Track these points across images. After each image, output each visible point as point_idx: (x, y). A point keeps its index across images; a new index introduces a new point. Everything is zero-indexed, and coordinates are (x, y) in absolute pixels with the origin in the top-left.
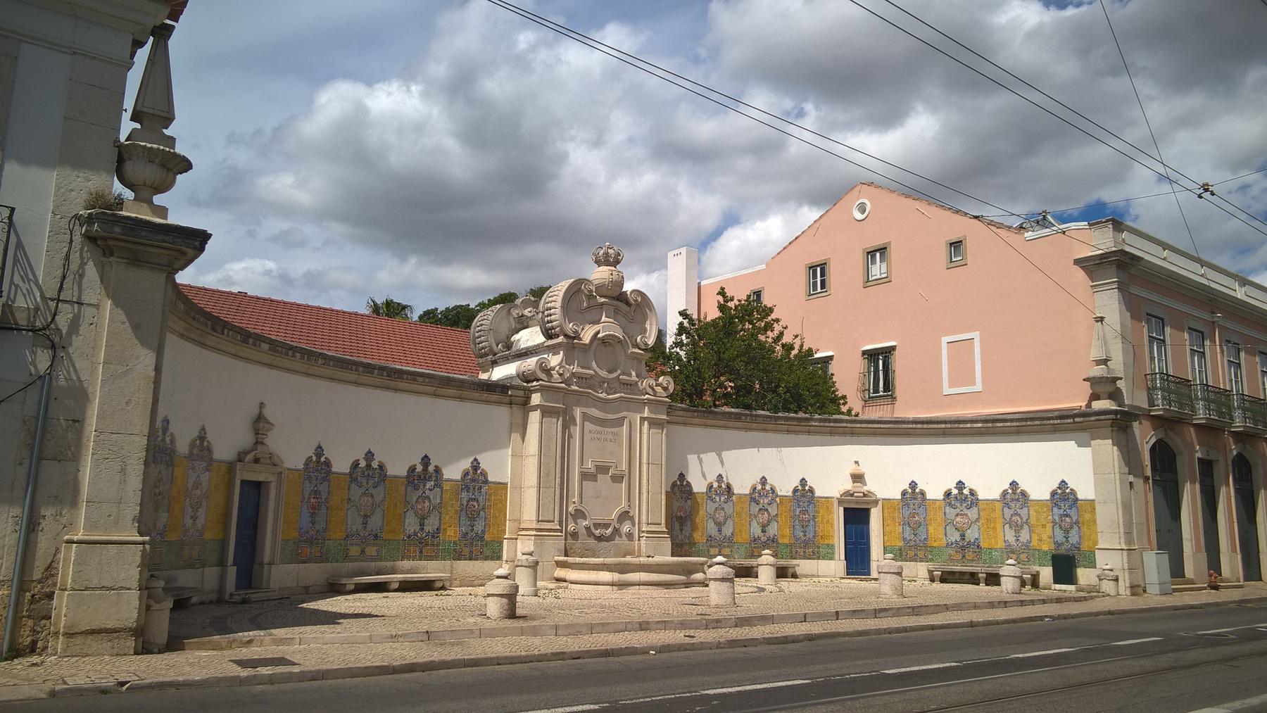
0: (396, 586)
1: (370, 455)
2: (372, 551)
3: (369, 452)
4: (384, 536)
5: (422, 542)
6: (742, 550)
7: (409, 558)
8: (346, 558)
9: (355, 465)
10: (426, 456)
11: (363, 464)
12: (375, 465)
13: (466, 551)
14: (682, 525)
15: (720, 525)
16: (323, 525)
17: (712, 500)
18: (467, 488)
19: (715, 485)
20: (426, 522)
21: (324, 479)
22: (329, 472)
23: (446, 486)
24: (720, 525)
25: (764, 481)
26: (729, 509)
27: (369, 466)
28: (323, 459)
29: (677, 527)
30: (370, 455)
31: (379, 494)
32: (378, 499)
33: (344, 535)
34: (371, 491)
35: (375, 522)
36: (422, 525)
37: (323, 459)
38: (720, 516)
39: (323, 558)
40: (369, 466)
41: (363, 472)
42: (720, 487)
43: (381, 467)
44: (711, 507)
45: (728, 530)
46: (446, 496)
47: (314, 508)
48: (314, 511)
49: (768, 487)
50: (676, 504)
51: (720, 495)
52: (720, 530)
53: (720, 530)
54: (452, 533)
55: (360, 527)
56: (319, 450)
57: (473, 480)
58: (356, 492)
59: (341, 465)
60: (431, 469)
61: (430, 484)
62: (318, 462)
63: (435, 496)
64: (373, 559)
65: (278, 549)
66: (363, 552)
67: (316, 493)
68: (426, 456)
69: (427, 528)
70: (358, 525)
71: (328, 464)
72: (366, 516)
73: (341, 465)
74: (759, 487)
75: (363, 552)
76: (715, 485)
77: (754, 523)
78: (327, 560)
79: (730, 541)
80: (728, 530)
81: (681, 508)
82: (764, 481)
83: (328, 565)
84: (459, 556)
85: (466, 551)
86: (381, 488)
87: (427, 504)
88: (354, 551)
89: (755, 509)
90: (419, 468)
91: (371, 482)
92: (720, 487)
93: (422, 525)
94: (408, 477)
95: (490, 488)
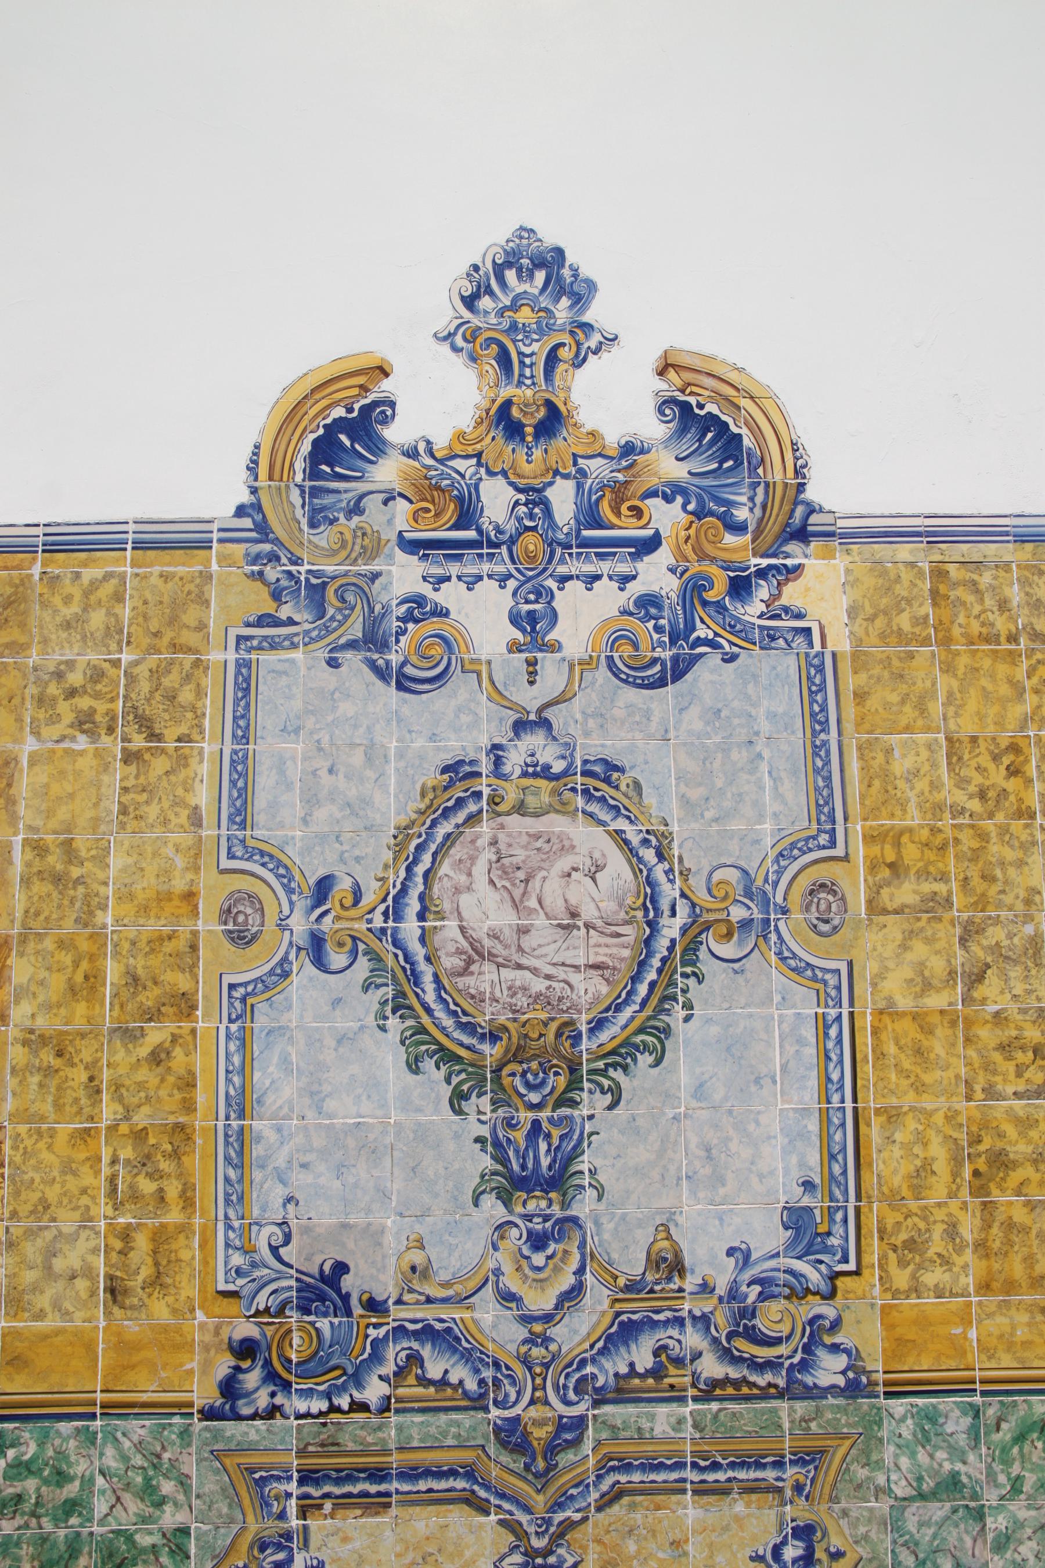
15: (531, 1087)
17: (405, 655)
24: (531, 1087)
26: (721, 766)
38: (535, 911)
42: (530, 424)
51: (535, 559)
52: (535, 1178)
53: (535, 1178)
76: (438, 401)
80: (710, 1153)
92: (530, 424)
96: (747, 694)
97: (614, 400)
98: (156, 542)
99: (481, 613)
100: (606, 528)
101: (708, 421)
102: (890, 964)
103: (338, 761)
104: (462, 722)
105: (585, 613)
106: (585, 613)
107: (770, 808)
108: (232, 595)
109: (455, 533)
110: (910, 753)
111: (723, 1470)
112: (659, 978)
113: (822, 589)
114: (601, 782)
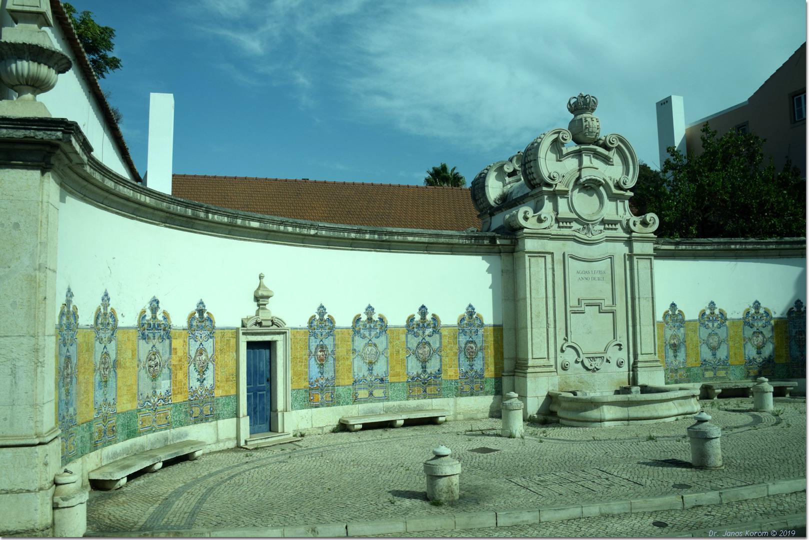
0: (402, 422)
1: (370, 310)
2: (378, 393)
3: (370, 307)
4: (389, 379)
5: (425, 383)
6: (738, 372)
7: (414, 397)
8: (356, 400)
9: (357, 319)
10: (423, 307)
11: (364, 318)
12: (375, 317)
13: (467, 388)
14: (675, 351)
15: (714, 350)
16: (332, 374)
17: (707, 327)
18: (464, 332)
19: (708, 312)
20: (428, 365)
21: (329, 334)
22: (332, 328)
23: (445, 332)
25: (757, 305)
26: (722, 333)
27: (370, 319)
28: (326, 317)
29: (671, 353)
31: (382, 342)
32: (381, 348)
33: (352, 381)
34: (374, 340)
35: (380, 368)
36: (424, 368)
37: (326, 317)
38: (714, 341)
39: (334, 401)
40: (370, 319)
41: (365, 326)
42: (713, 313)
43: (382, 319)
44: (704, 333)
45: (722, 354)
46: (445, 341)
47: (321, 360)
48: (321, 363)
49: (762, 311)
50: (669, 333)
51: (713, 321)
52: (714, 355)
53: (714, 355)
54: (451, 373)
55: (366, 374)
56: (322, 310)
57: (469, 325)
59: (343, 321)
60: (429, 317)
61: (428, 331)
62: (321, 320)
63: (435, 342)
64: (380, 400)
65: (290, 399)
66: (371, 394)
67: (323, 348)
68: (423, 307)
69: (429, 370)
70: (365, 371)
71: (331, 320)
72: (371, 364)
73: (343, 321)
74: (753, 311)
75: (371, 394)
76: (708, 312)
77: (749, 346)
78: (338, 404)
79: (725, 364)
80: (722, 354)
81: (674, 336)
82: (757, 305)
83: (340, 408)
84: (461, 393)
85: (467, 388)
86: (383, 338)
87: (427, 349)
88: (363, 394)
89: (749, 332)
90: (418, 317)
91: (373, 333)
92: (713, 313)
93: (424, 368)
94: (408, 326)
95: (486, 331)
96: (723, 329)
97: (717, 312)
98: (694, 321)
99: (710, 325)
100: (716, 320)
101: (722, 313)
102: (731, 343)
103: (704, 333)
104: (710, 331)
105: (716, 324)
106: (716, 324)
107: (725, 335)
108: (698, 324)
109: (709, 320)
110: (732, 332)
111: (723, 369)
112: (720, 344)
113: (727, 323)
114: (716, 334)
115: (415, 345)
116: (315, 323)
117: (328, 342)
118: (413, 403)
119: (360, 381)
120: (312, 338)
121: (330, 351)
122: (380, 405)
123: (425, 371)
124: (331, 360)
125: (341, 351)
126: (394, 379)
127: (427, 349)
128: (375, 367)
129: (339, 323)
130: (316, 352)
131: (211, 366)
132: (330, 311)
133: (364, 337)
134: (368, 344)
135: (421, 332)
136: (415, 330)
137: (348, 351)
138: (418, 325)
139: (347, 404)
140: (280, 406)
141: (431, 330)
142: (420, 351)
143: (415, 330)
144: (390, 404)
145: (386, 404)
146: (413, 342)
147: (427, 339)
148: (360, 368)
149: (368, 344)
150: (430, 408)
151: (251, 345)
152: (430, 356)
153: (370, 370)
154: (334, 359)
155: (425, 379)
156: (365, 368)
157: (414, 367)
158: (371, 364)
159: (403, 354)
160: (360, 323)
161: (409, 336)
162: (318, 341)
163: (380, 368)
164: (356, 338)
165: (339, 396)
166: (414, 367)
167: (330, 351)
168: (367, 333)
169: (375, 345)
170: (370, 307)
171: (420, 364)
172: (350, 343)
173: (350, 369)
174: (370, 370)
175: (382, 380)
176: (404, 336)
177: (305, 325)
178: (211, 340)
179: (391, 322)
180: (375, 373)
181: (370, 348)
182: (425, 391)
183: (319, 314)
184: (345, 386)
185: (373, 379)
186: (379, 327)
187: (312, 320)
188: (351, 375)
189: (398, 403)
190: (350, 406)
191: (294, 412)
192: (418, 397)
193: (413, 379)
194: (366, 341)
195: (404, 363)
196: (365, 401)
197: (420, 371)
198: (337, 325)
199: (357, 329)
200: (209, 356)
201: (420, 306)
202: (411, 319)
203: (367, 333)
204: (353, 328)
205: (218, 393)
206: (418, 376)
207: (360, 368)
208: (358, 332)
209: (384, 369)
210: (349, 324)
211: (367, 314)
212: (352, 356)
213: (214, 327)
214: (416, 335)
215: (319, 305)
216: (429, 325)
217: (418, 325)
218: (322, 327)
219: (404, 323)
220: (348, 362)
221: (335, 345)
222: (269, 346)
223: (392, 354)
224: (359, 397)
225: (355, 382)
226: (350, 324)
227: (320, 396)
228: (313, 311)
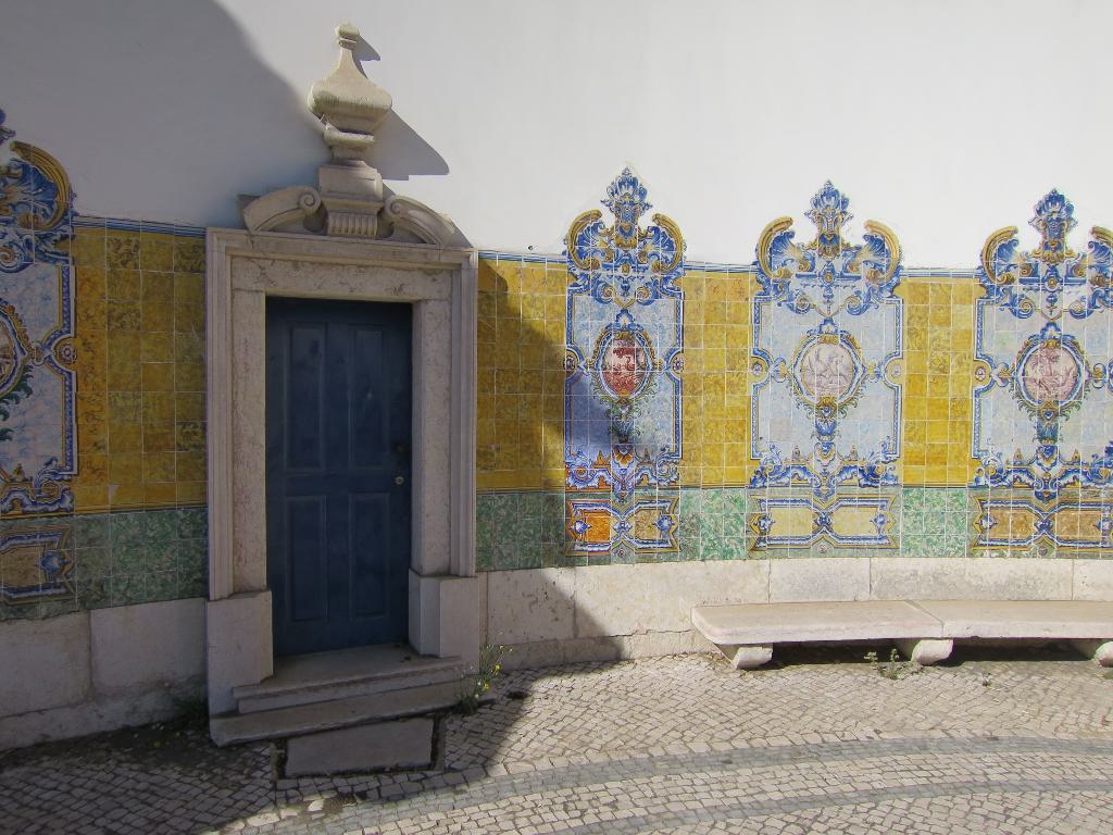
0: (944, 649)
1: (830, 205)
2: (853, 521)
3: (829, 193)
4: (899, 470)
7: (998, 546)
8: (761, 543)
9: (777, 239)
11: (806, 233)
21: (657, 291)
22: (672, 266)
27: (829, 241)
28: (645, 222)
30: (830, 205)
31: (877, 331)
34: (844, 322)
35: (868, 429)
36: (1048, 439)
37: (645, 222)
40: (829, 241)
55: (809, 446)
56: (629, 193)
58: (783, 330)
61: (1071, 296)
62: (625, 231)
64: (856, 545)
66: (823, 523)
68: (1055, 198)
69: (1066, 449)
71: (665, 234)
73: (719, 238)
75: (823, 523)
78: (690, 553)
83: (693, 568)
86: (882, 316)
87: (1065, 362)
88: (789, 521)
90: (1030, 241)
91: (842, 294)
93: (1048, 439)
94: (986, 272)
115: (1016, 346)
116: (598, 242)
117: (657, 319)
118: (992, 568)
119: (780, 472)
120: (584, 299)
121: (660, 352)
122: (861, 566)
123: (1051, 450)
124: (662, 389)
125: (706, 357)
126: (922, 474)
127: (1065, 362)
128: (844, 424)
129: (696, 249)
130: (599, 354)
131: (48, 384)
132: (662, 201)
133: (802, 308)
134: (821, 335)
135: (1040, 299)
136: (1018, 288)
137: (734, 360)
138: (1031, 270)
139: (727, 554)
140: (430, 546)
141: (1085, 291)
142: (1035, 373)
143: (1018, 288)
144: (902, 564)
145: (882, 562)
146: (1006, 335)
147: (1067, 325)
148: (782, 425)
149: (821, 335)
150: (1064, 593)
151: (280, 310)
152: (1076, 392)
153: (826, 434)
154: (678, 386)
155: (1046, 483)
156: (805, 423)
157: (1005, 432)
158: (827, 408)
159: (961, 383)
160: (788, 253)
161: (992, 312)
162: (610, 313)
163: (868, 429)
164: (772, 309)
165: (694, 525)
166: (1005, 432)
167: (660, 352)
168: (815, 294)
169: (849, 341)
170: (829, 193)
171: (1029, 424)
172: (747, 327)
173: (744, 423)
174: (826, 434)
175: (871, 475)
176: (970, 310)
177: (552, 243)
178: (51, 270)
179: (917, 253)
180: (842, 446)
181: (826, 351)
182: (1046, 527)
183: (618, 210)
184: (718, 487)
185: (834, 468)
186: (864, 271)
187: (582, 232)
188: (745, 449)
189: (933, 563)
190: (737, 566)
191: (496, 577)
192: (1019, 547)
193: (998, 476)
194: (813, 321)
195: (960, 416)
196: (799, 547)
197: (1030, 448)
198: (690, 254)
199: (774, 274)
200: (37, 336)
201: (1041, 194)
202: (1002, 245)
203: (815, 294)
204: (760, 269)
205: (85, 496)
206: (1022, 468)
207: (782, 425)
208: (781, 287)
209: (883, 433)
210: (744, 253)
211: (820, 219)
212: (750, 377)
213: (66, 215)
214: (1019, 309)
215: (615, 174)
216: (1076, 270)
217: (1031, 270)
218: (627, 261)
219: (971, 261)
220: (729, 401)
221: (681, 332)
222: (397, 318)
223: (915, 379)
224: (775, 532)
225: (761, 474)
226: (746, 255)
227: (614, 523)
228: (590, 195)
